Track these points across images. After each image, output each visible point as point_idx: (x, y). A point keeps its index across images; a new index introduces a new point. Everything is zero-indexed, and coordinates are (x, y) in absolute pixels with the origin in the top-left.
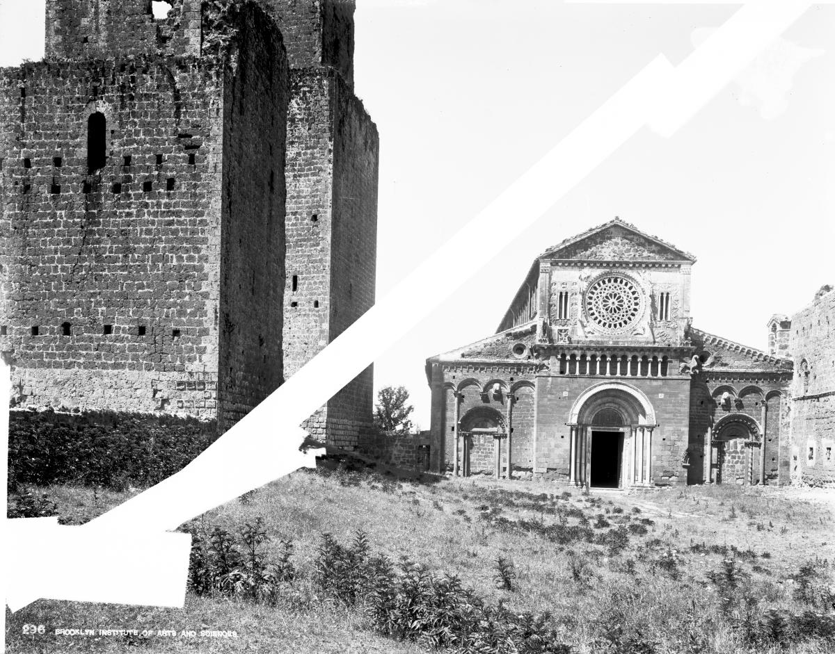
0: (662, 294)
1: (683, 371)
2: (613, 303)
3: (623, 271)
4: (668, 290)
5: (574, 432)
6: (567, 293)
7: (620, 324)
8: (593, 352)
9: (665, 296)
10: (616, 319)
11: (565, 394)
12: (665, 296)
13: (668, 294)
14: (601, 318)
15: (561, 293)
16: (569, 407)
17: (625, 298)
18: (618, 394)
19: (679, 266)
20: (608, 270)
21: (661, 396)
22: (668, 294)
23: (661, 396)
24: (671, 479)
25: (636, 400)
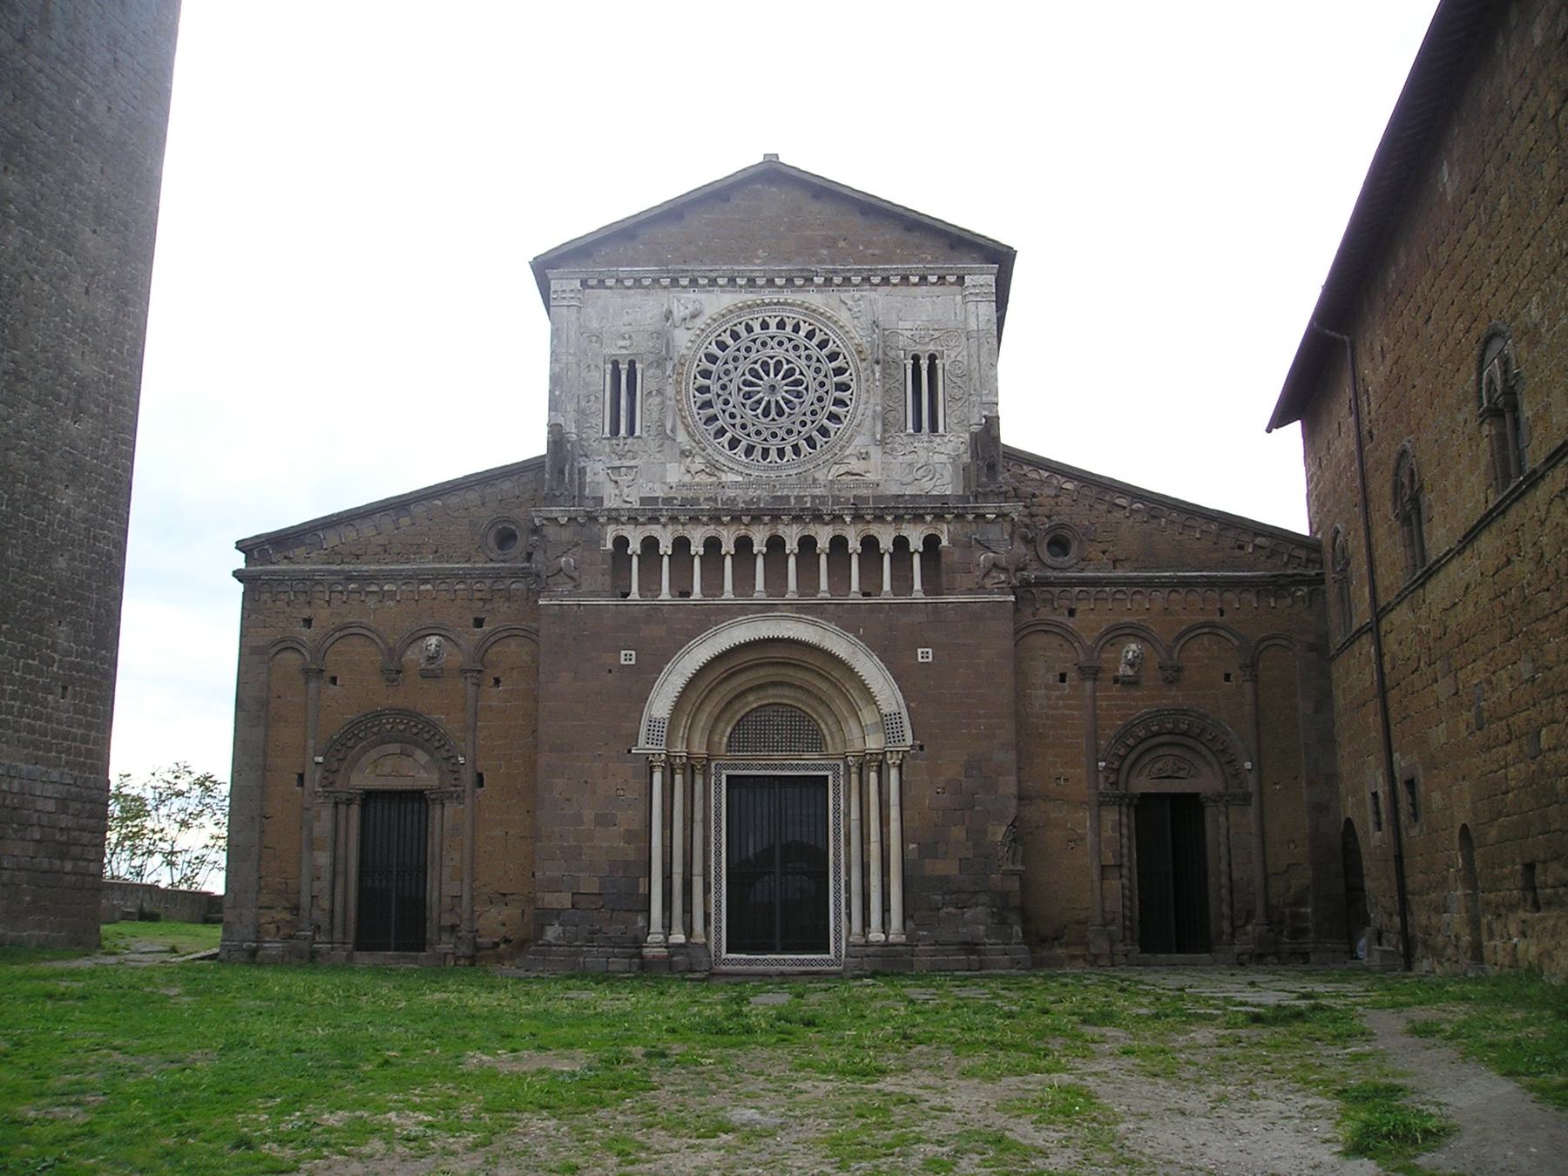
0: (916, 358)
1: (986, 575)
2: (773, 388)
3: (799, 297)
4: (932, 348)
5: (657, 777)
6: (632, 364)
7: (796, 450)
8: (711, 531)
9: (924, 364)
10: (782, 433)
11: (627, 657)
12: (924, 364)
13: (932, 358)
14: (739, 433)
15: (615, 364)
16: (643, 698)
17: (810, 374)
18: (796, 655)
19: (960, 280)
20: (750, 297)
21: (925, 655)
22: (932, 358)
23: (925, 655)
24: (969, 914)
25: (850, 670)
